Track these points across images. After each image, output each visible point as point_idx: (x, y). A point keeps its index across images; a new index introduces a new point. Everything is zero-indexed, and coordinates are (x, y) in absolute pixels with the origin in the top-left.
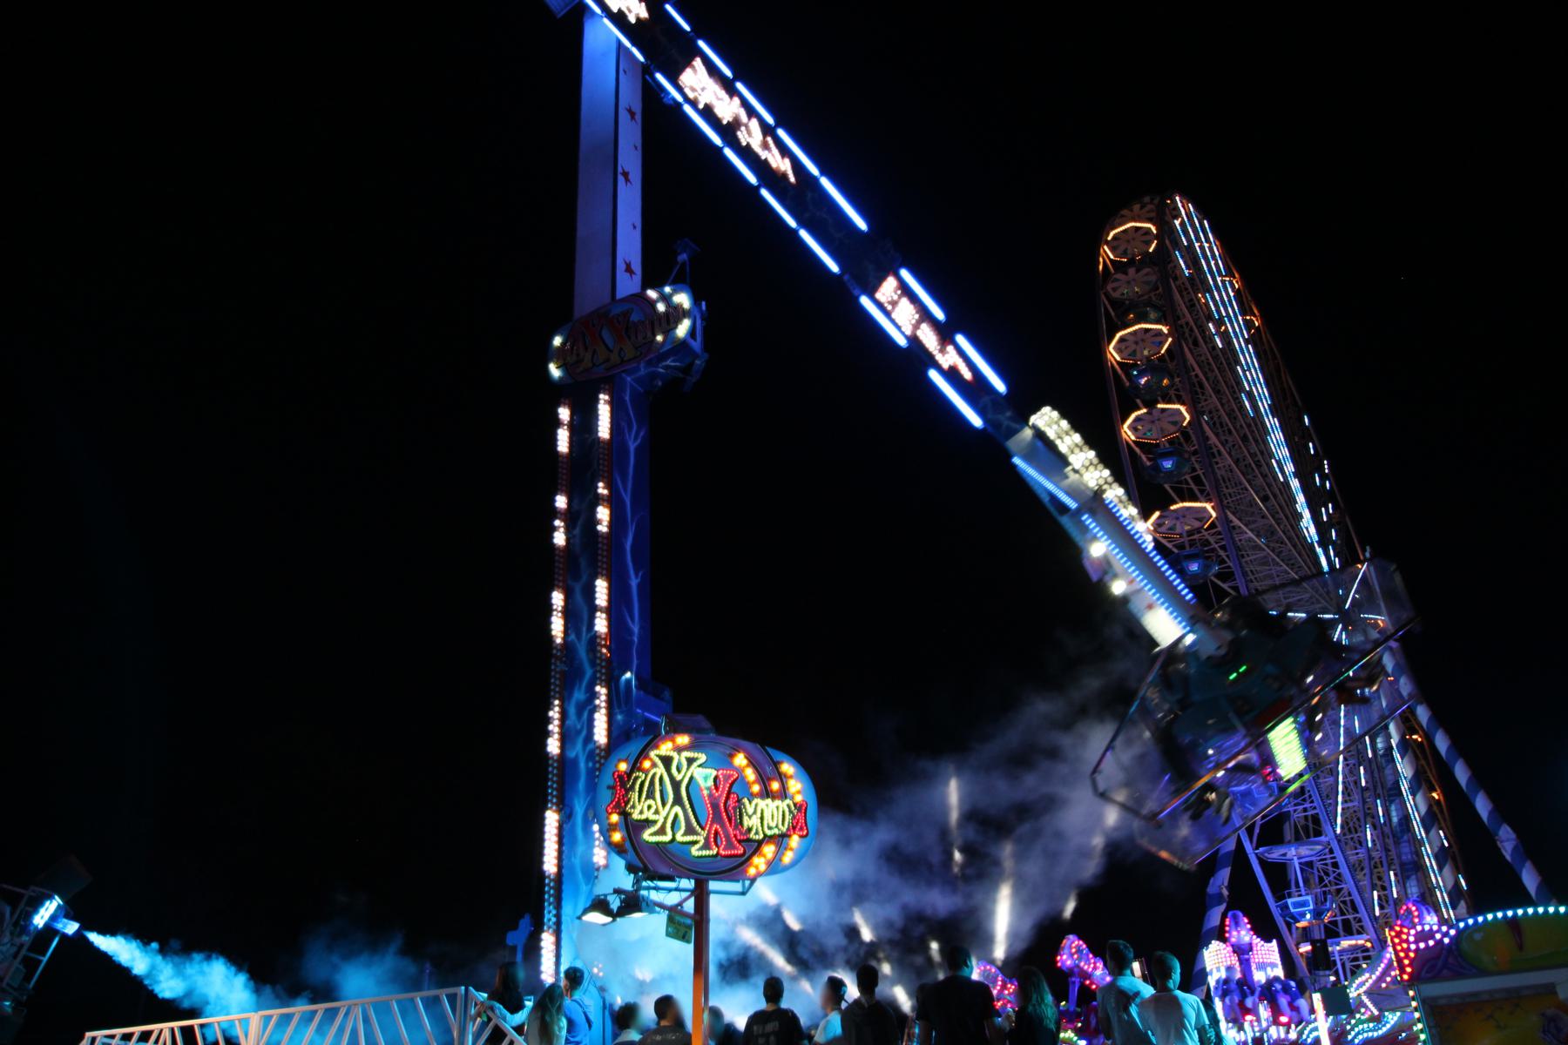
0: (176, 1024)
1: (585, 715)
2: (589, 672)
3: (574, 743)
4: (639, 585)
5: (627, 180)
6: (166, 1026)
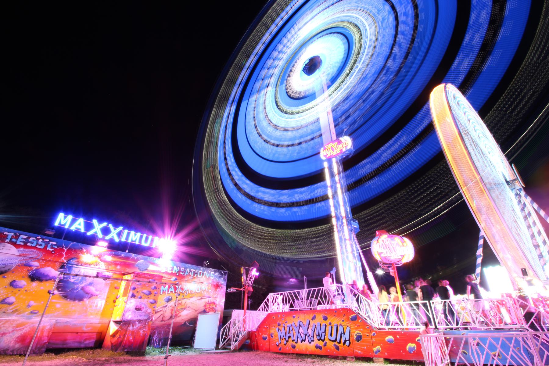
0: (288, 292)
1: (342, 227)
2: (341, 218)
3: (340, 233)
4: (347, 199)
5: (329, 114)
6: (286, 292)
